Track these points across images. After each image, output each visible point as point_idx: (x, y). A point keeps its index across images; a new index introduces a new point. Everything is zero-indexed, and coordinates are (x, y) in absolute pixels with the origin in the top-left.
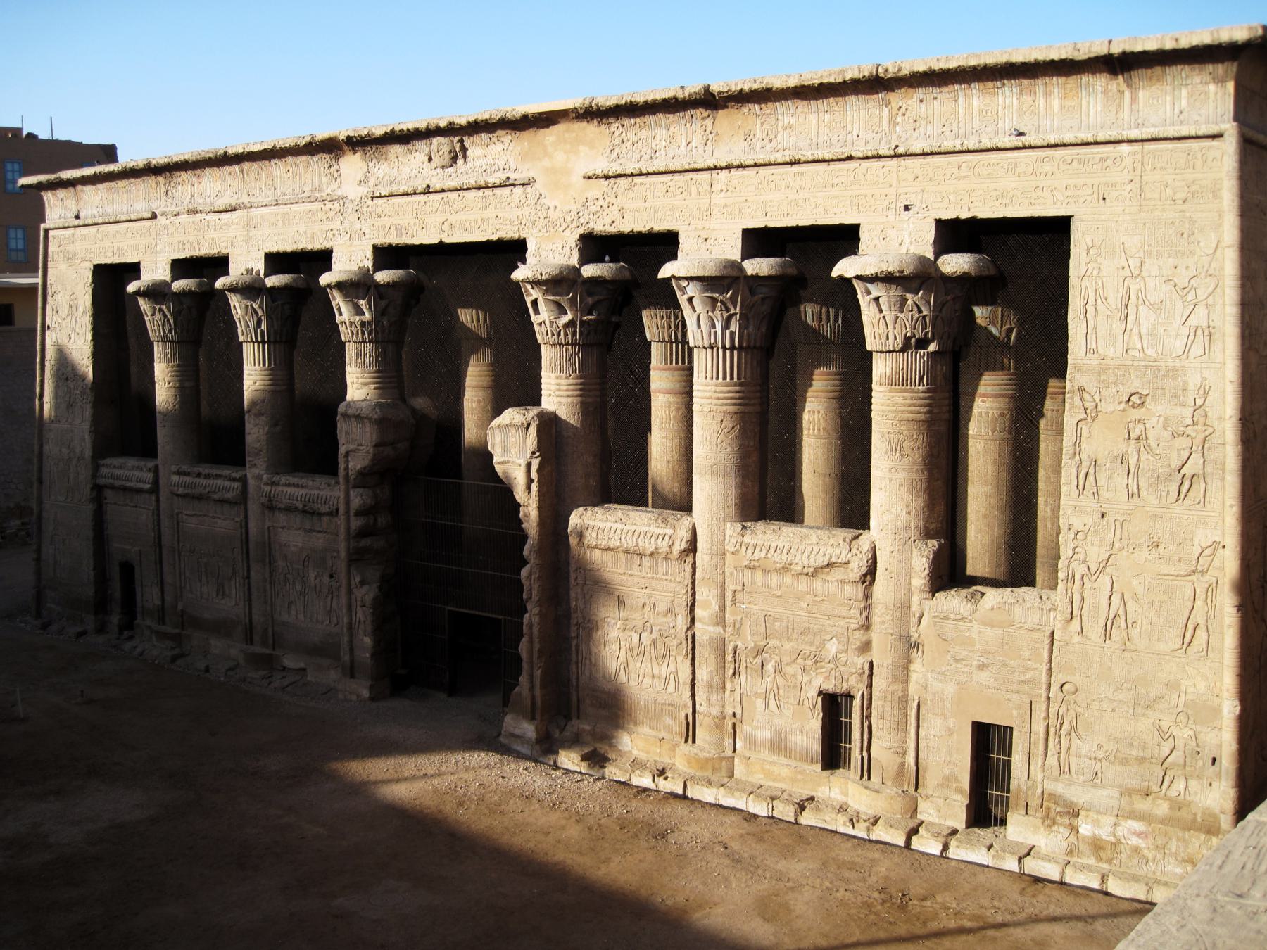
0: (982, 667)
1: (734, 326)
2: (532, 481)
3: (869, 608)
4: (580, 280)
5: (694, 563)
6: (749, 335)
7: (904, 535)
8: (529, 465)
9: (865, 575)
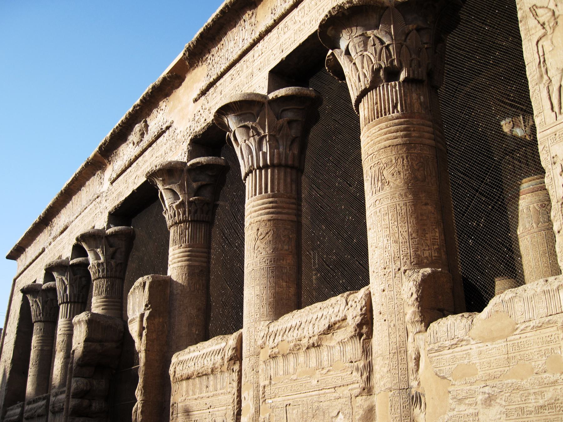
0: (489, 400)
1: (266, 148)
2: (144, 328)
3: (369, 368)
4: (185, 169)
5: (240, 371)
6: (279, 154)
7: (393, 267)
8: (142, 315)
9: (359, 326)
